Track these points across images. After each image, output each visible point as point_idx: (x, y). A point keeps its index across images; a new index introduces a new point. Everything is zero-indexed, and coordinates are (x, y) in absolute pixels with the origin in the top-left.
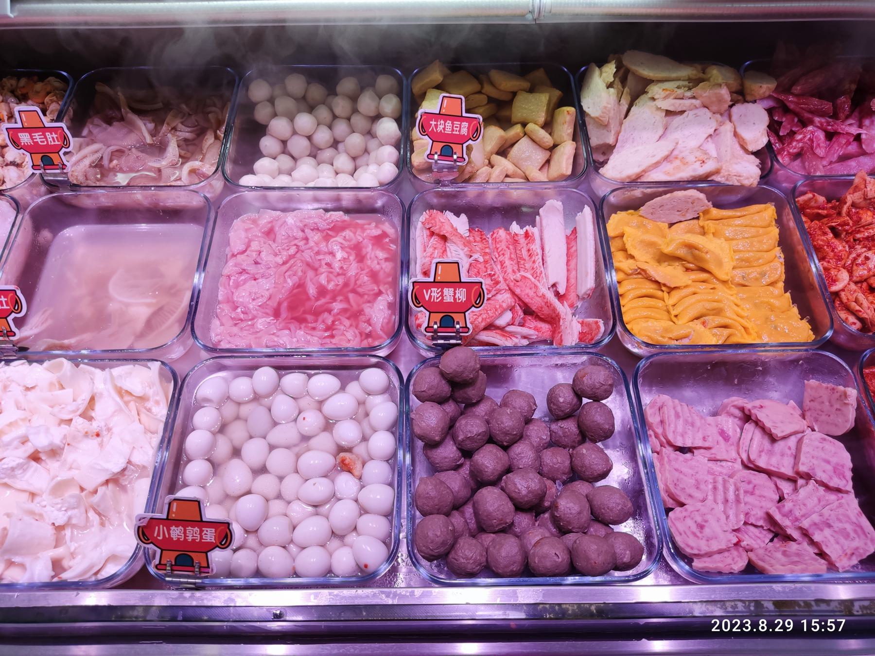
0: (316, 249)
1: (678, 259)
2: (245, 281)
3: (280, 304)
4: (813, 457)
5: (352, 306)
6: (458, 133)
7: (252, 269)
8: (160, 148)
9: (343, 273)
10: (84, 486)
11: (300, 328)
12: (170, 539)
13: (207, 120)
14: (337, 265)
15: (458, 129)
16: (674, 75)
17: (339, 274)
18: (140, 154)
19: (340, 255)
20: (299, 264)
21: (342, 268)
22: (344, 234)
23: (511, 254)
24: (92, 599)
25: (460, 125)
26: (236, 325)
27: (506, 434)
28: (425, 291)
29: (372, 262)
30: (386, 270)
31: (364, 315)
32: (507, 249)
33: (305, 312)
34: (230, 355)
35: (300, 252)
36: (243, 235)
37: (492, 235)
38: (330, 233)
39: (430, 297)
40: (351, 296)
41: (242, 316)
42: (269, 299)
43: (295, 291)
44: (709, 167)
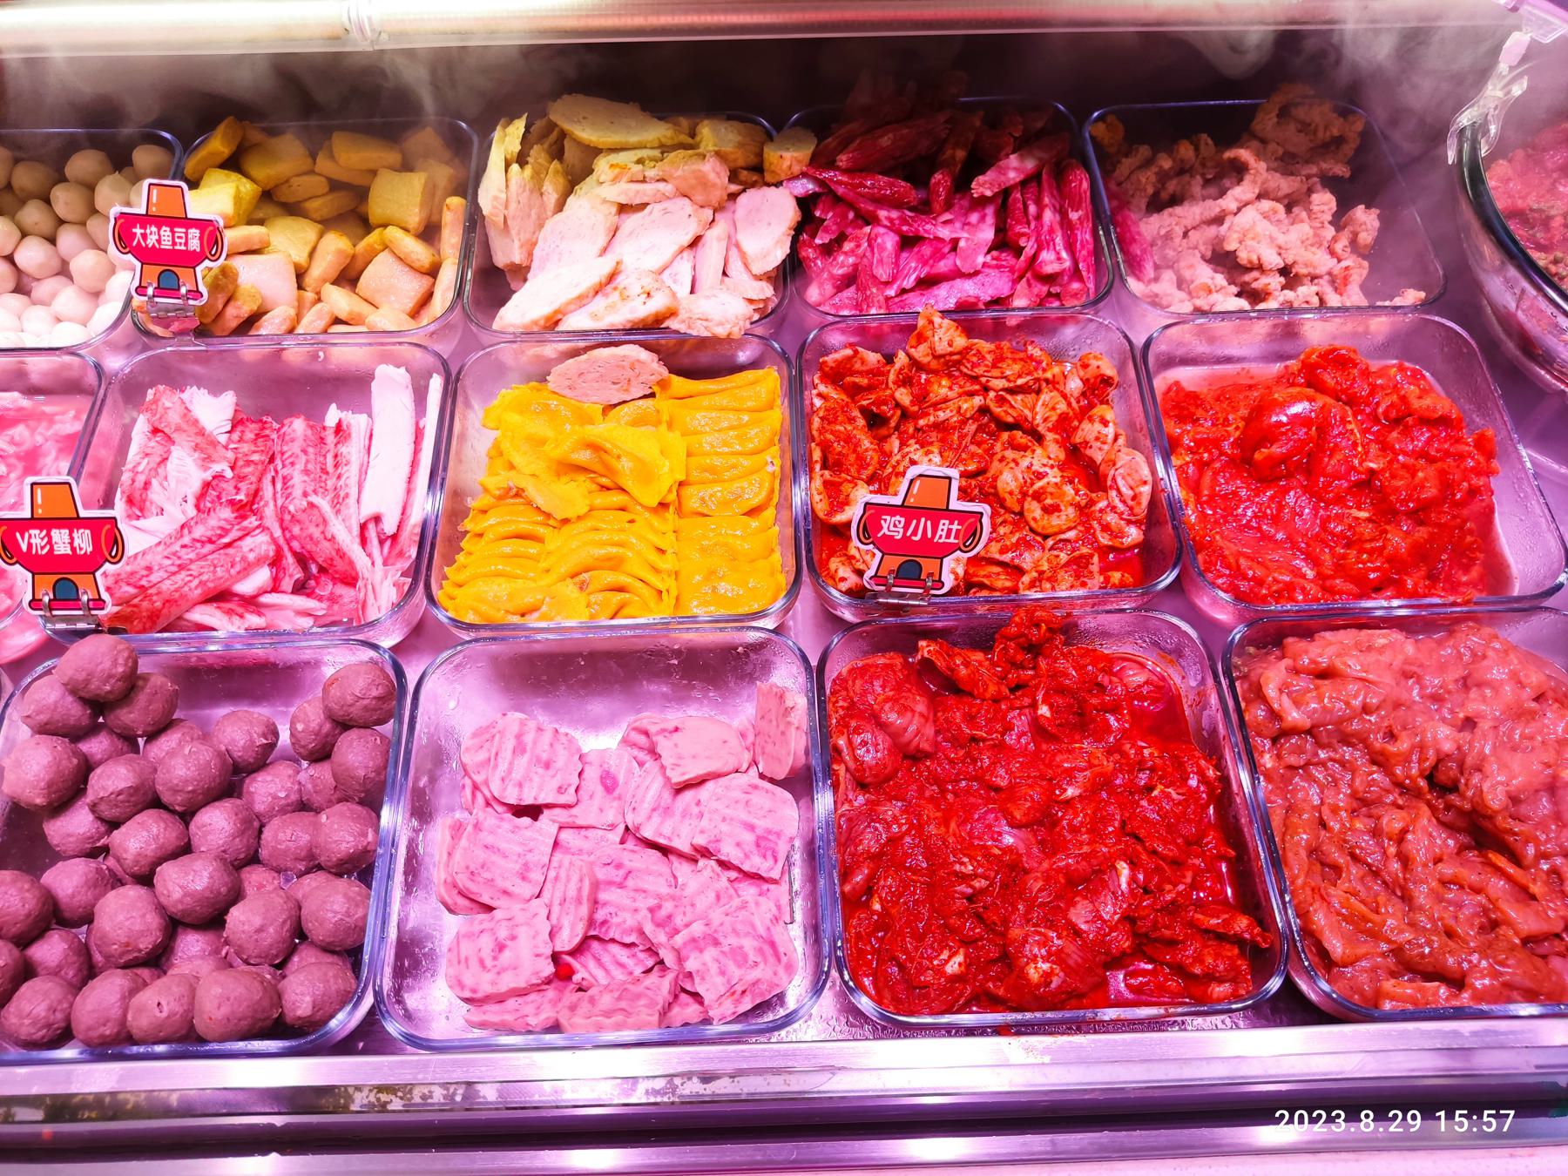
1: (582, 469)
4: (724, 819)
6: (183, 248)
15: (183, 241)
16: (633, 139)
23: (307, 462)
25: (186, 234)
27: (176, 791)
44: (657, 304)
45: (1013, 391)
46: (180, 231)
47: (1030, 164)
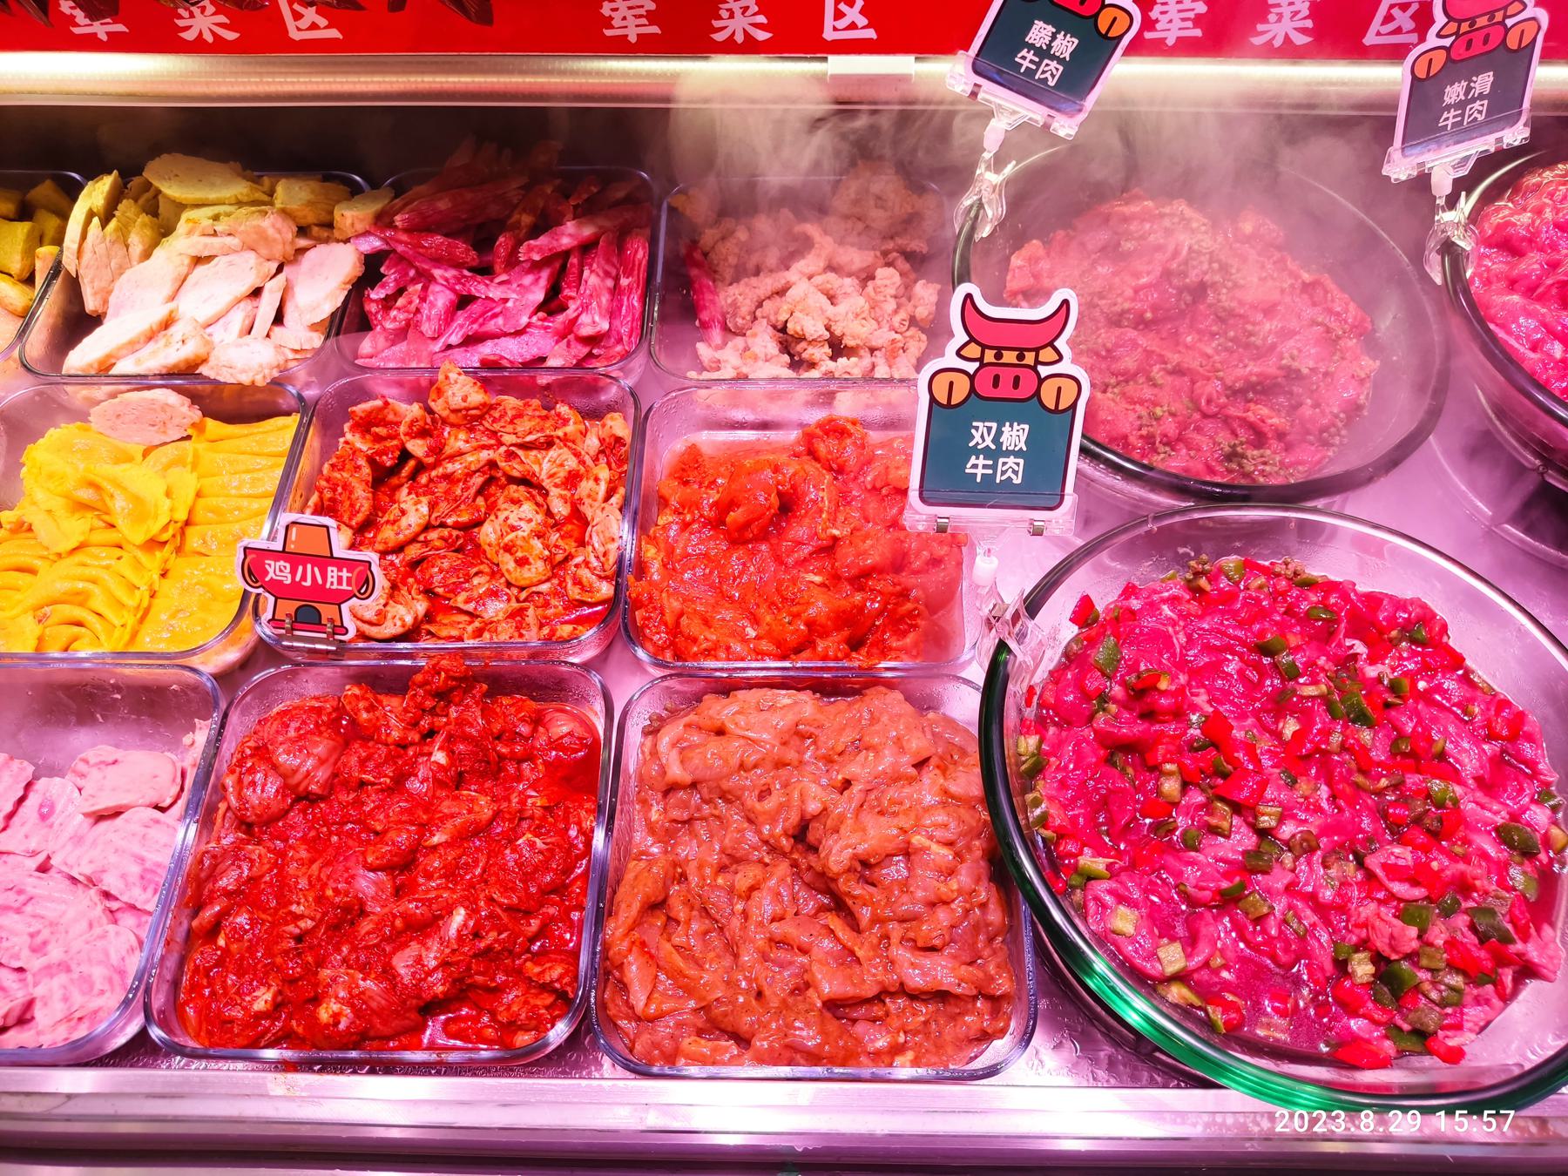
4: (116, 851)
16: (212, 195)
45: (526, 447)
47: (588, 231)
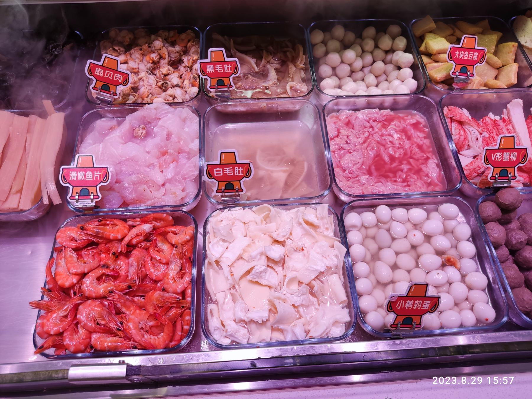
0: (380, 133)
2: (344, 154)
3: (370, 167)
5: (413, 166)
6: (471, 59)
7: (346, 146)
8: (263, 75)
9: (401, 147)
10: (302, 281)
11: (387, 182)
12: (404, 307)
13: (286, 56)
14: (397, 142)
15: (472, 57)
17: (399, 148)
18: (254, 78)
19: (396, 136)
20: (373, 142)
21: (400, 144)
22: (394, 123)
23: (496, 132)
24: (462, 340)
25: (473, 54)
26: (348, 180)
28: (492, 155)
29: (417, 139)
30: (427, 144)
31: (423, 172)
32: (493, 129)
33: (386, 172)
34: (362, 198)
35: (371, 136)
36: (334, 126)
37: (483, 121)
38: (385, 123)
39: (495, 158)
40: (411, 160)
41: (350, 175)
42: (363, 164)
43: (376, 159)
46: (471, 53)
